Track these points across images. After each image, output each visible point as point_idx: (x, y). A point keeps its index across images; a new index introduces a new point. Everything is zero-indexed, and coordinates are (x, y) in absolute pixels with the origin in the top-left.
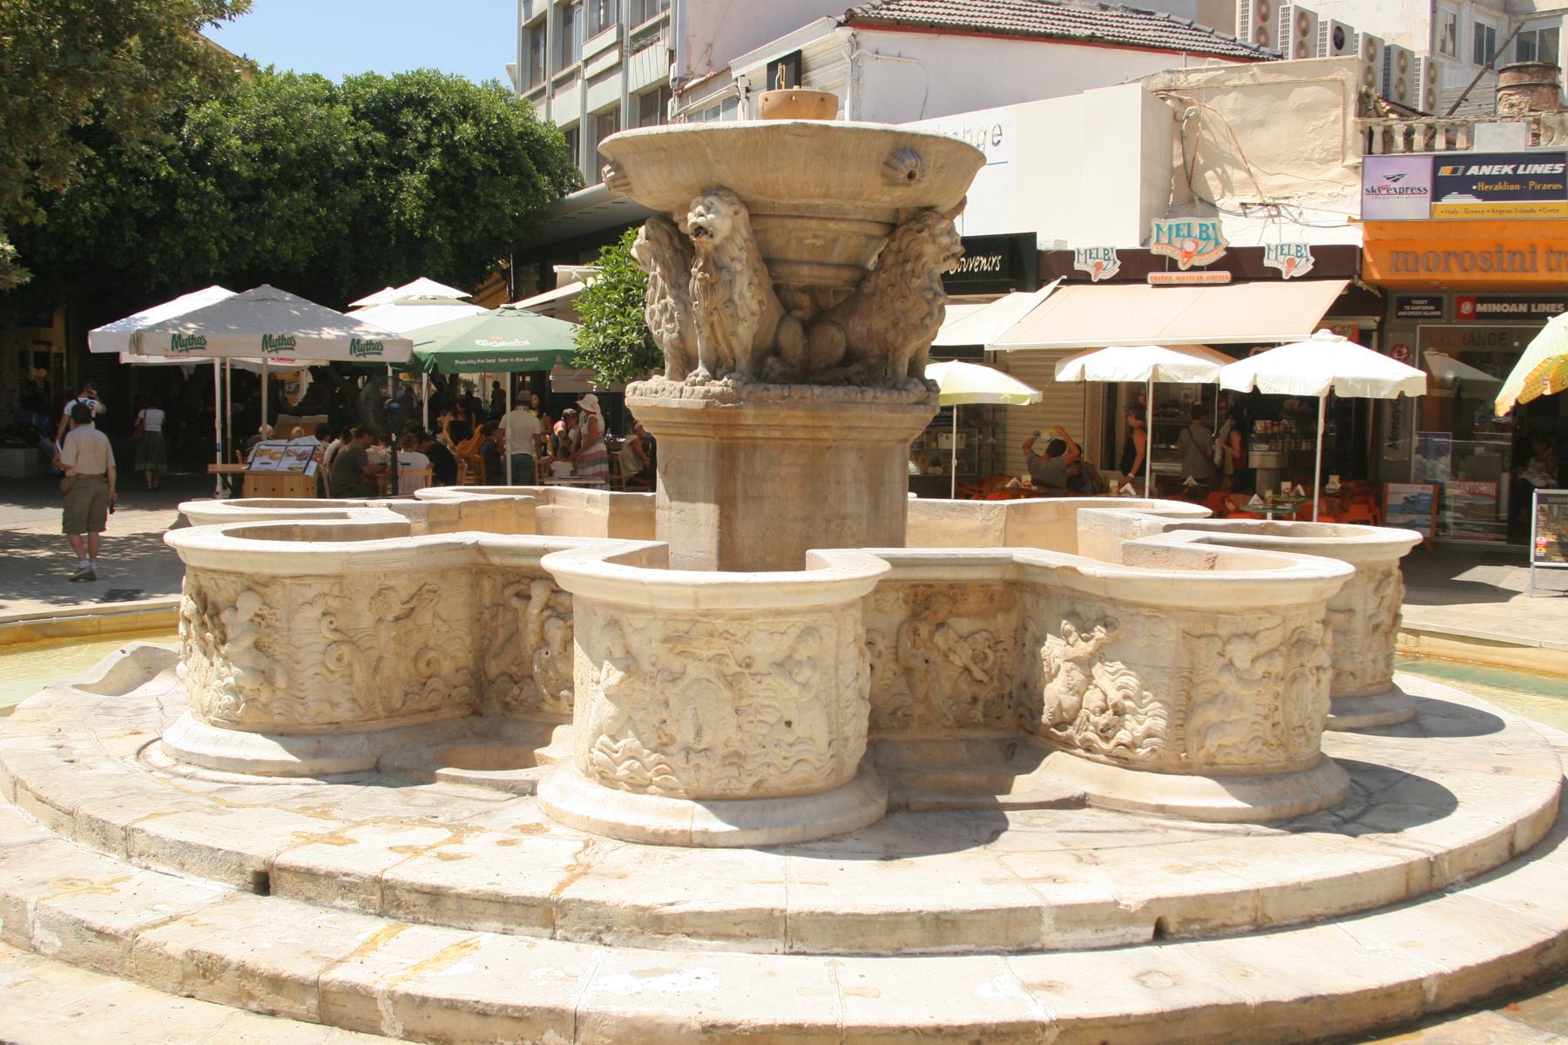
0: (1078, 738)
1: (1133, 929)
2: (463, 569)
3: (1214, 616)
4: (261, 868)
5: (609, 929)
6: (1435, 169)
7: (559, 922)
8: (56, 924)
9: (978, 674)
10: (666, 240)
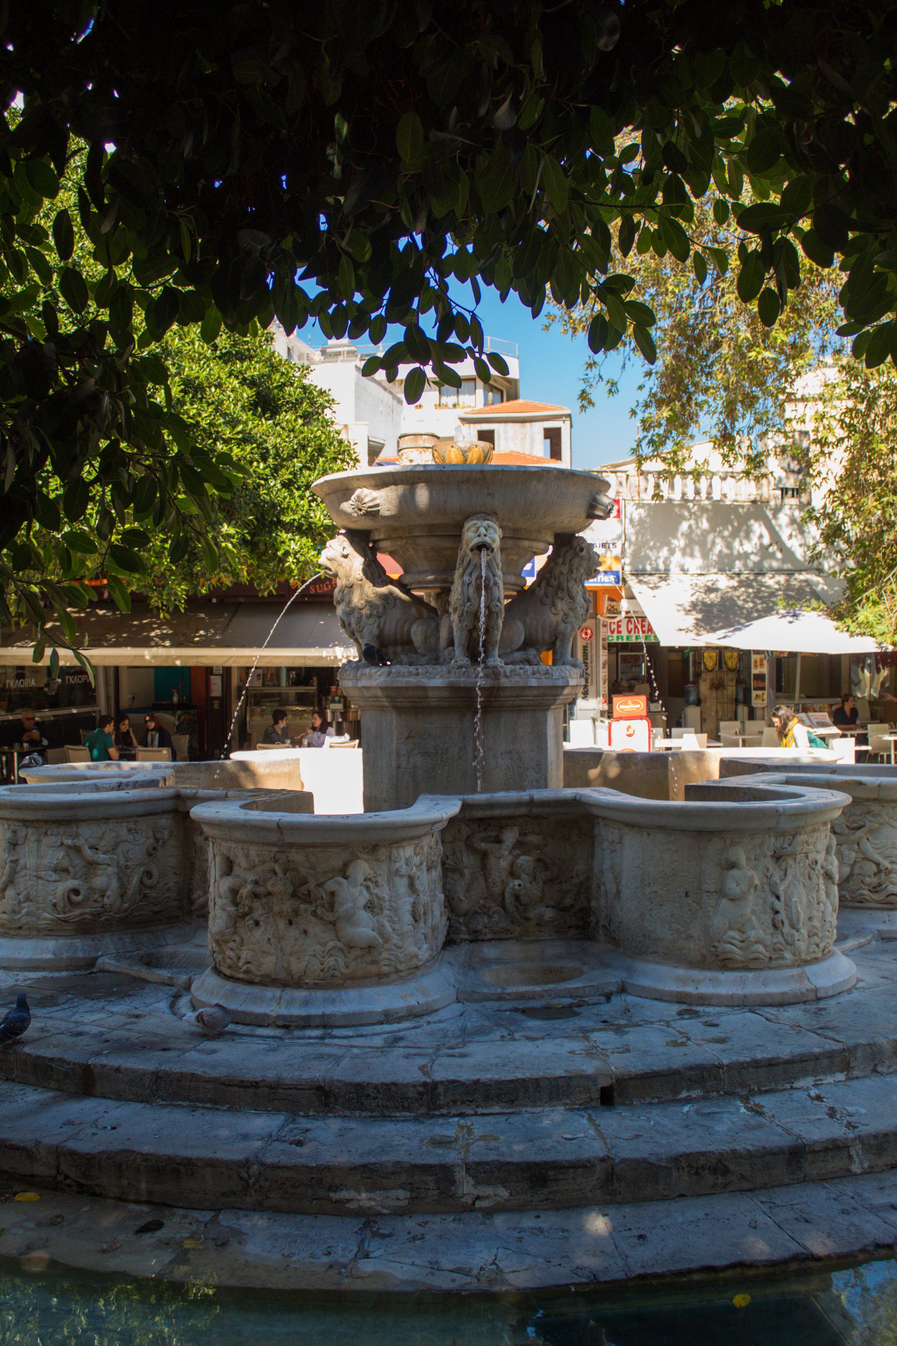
4: (604, 1082)
7: (852, 1065)
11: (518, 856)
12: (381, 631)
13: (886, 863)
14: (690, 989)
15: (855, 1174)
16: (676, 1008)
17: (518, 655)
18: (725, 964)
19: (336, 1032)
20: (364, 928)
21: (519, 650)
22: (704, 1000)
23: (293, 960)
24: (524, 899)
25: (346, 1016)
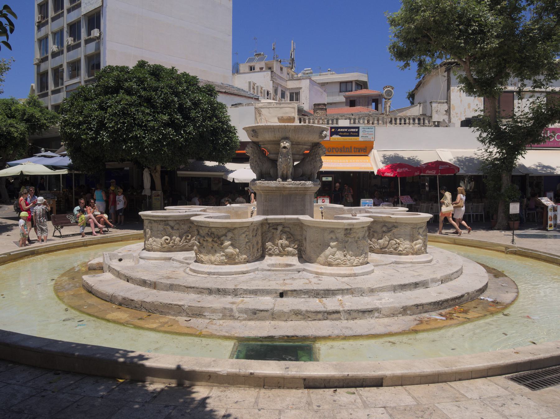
3: (416, 224)
6: (331, 130)
8: (241, 311)
10: (256, 148)
12: (261, 171)
14: (319, 271)
16: (315, 275)
18: (330, 265)
22: (322, 274)
24: (283, 245)
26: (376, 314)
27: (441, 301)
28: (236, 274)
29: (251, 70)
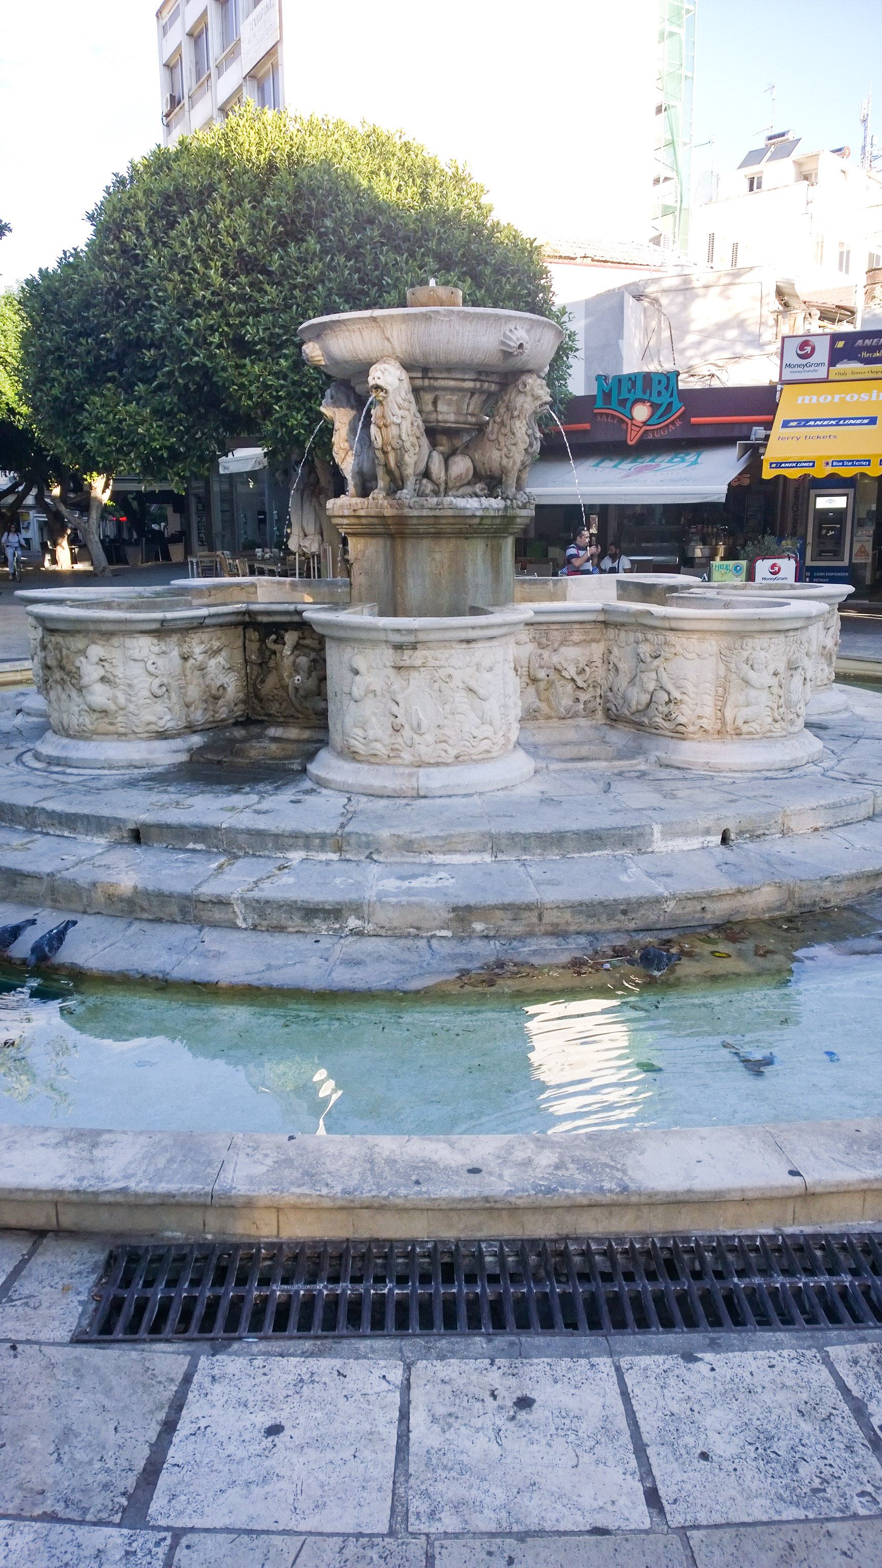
0: (646, 721)
1: (709, 838)
2: (236, 625)
5: (378, 852)
7: (345, 848)
9: (580, 683)
11: (298, 656)
13: (676, 694)
15: (239, 928)
17: (468, 489)
19: (69, 770)
20: (99, 695)
21: (469, 484)
23: (65, 716)
25: (78, 759)
26: (353, 922)
27: (628, 902)
28: (110, 768)
29: (751, 189)
